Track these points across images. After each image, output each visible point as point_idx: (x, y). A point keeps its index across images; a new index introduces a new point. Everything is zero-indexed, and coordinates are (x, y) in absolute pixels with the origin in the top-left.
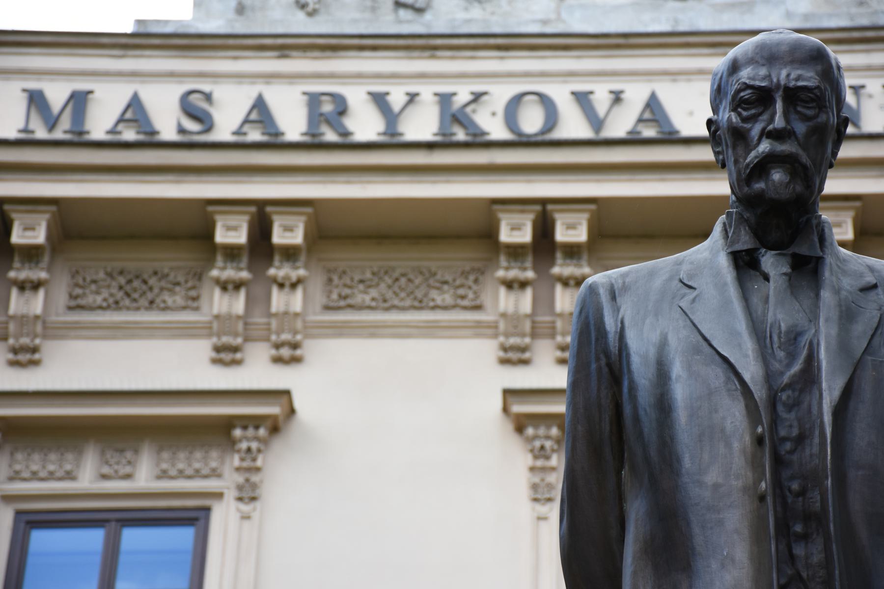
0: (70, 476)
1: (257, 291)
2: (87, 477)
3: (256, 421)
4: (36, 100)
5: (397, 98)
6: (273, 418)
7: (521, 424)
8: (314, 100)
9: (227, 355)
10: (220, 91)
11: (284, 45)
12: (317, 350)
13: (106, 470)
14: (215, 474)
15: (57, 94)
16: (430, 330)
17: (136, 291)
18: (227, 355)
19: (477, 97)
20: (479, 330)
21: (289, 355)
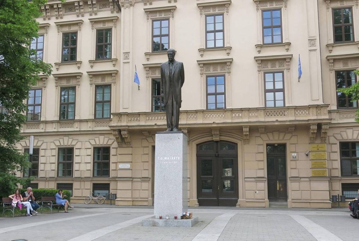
0: (156, 16)
2: (158, 16)
3: (173, 9)
6: (174, 9)
7: (199, 7)
13: (159, 15)
14: (170, 15)
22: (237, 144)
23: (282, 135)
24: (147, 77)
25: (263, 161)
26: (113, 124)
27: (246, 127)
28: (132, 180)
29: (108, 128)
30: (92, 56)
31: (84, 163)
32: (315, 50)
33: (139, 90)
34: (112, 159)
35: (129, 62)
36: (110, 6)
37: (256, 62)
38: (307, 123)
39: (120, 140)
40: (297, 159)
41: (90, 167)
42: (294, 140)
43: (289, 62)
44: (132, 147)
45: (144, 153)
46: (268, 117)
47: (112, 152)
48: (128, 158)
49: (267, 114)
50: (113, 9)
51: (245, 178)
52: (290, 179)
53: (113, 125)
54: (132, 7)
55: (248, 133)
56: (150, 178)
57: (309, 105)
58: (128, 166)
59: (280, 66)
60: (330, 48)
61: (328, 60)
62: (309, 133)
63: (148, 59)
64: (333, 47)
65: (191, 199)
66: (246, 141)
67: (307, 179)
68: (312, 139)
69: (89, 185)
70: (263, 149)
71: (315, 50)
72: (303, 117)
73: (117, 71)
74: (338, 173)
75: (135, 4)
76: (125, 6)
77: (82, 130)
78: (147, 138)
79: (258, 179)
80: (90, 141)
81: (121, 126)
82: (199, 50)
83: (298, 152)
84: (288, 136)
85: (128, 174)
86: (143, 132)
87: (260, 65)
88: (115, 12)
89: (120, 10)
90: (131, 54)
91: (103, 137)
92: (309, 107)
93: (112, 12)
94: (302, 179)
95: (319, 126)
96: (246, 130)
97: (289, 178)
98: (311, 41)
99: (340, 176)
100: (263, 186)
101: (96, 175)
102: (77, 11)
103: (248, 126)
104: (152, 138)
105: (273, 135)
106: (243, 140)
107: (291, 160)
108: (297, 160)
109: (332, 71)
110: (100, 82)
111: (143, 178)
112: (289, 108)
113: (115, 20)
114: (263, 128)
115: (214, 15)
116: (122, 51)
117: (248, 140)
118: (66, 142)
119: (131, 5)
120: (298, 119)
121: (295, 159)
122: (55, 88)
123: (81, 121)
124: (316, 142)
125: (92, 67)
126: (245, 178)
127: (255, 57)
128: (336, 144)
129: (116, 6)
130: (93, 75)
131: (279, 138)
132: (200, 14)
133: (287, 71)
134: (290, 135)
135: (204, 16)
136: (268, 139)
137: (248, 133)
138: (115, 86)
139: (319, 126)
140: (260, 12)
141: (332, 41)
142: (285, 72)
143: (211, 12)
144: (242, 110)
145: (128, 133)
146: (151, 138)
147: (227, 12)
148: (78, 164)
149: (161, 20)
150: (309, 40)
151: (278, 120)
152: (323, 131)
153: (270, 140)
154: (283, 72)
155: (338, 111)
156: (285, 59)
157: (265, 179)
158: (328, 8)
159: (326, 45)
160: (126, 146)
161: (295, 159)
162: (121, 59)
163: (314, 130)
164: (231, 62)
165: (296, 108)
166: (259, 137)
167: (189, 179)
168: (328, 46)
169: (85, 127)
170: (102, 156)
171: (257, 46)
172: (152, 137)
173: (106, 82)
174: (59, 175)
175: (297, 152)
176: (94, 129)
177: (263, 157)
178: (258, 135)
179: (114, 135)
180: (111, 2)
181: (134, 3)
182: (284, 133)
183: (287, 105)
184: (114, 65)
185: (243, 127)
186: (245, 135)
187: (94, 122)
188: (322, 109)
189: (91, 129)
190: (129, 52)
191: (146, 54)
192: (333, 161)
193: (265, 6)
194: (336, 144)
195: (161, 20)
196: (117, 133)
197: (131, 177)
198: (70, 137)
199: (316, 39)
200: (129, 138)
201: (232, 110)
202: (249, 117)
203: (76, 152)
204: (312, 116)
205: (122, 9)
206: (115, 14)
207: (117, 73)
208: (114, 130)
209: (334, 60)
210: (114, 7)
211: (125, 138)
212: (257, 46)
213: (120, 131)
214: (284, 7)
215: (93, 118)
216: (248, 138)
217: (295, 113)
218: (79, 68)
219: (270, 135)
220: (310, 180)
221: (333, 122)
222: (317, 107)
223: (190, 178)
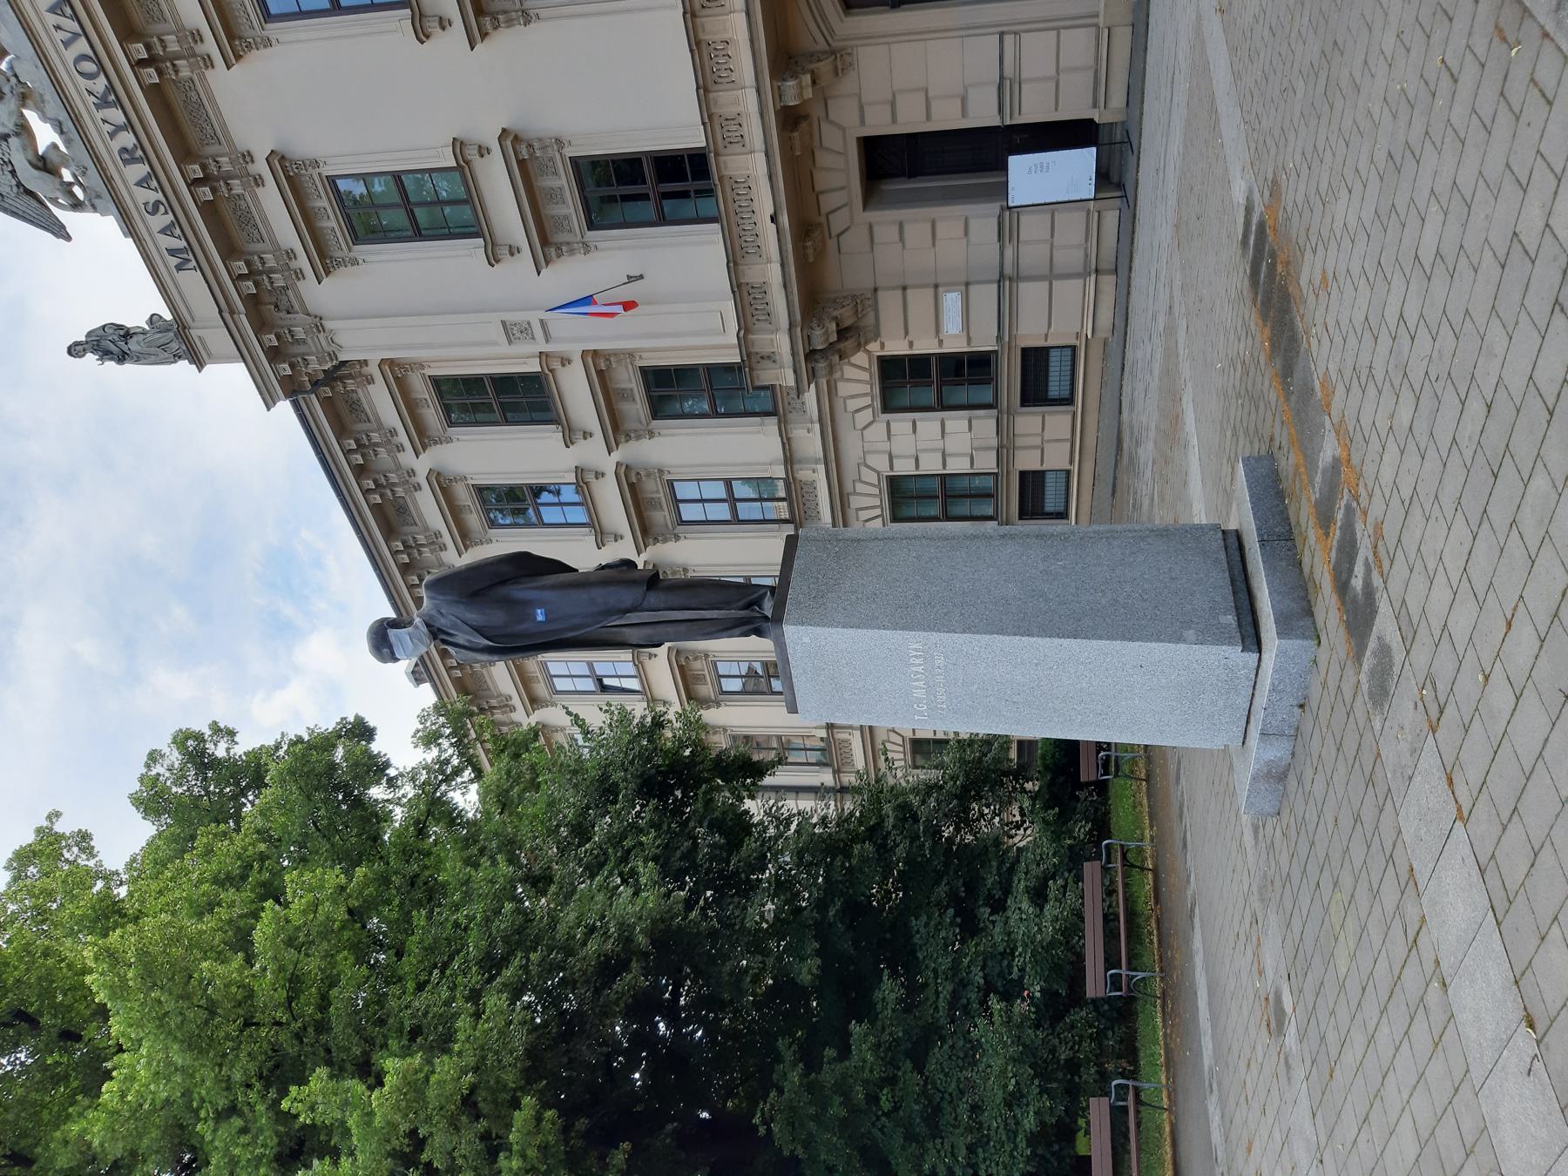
1: (227, 178)
4: (179, 268)
8: (126, 162)
9: (259, 181)
10: (141, 202)
11: (108, 181)
15: (173, 261)
16: (212, 100)
17: (246, 219)
18: (259, 181)
19: (90, 93)
21: (248, 157)
24: (586, 248)
26: (789, 380)
29: (810, 396)
30: (549, 437)
31: (948, 442)
33: (641, 277)
34: (925, 346)
35: (541, 321)
41: (957, 422)
44: (876, 290)
45: (897, 238)
47: (896, 347)
53: (791, 382)
54: (328, 325)
65: (1101, 21)
69: (1029, 422)
75: (311, 309)
76: (329, 349)
77: (821, 455)
80: (860, 425)
81: (794, 354)
85: (985, 297)
86: (811, 259)
90: (510, 317)
91: (840, 385)
101: (986, 394)
102: (400, 491)
110: (639, 405)
113: (397, 373)
116: (504, 348)
118: (869, 502)
119: (320, 328)
122: (682, 542)
123: (789, 460)
125: (587, 435)
130: (616, 429)
132: (269, 50)
135: (273, 29)
138: (644, 355)
148: (948, 460)
160: (872, 315)
167: (1006, 37)
169: (809, 441)
170: (911, 382)
173: (633, 385)
174: (990, 511)
176: (815, 417)
179: (831, 372)
187: (790, 416)
189: (817, 426)
190: (503, 323)
197: (995, 286)
198: (848, 487)
203: (904, 468)
205: (343, 357)
210: (350, 376)
213: (811, 355)
215: (774, 420)
218: (599, 475)
223: (1002, 34)
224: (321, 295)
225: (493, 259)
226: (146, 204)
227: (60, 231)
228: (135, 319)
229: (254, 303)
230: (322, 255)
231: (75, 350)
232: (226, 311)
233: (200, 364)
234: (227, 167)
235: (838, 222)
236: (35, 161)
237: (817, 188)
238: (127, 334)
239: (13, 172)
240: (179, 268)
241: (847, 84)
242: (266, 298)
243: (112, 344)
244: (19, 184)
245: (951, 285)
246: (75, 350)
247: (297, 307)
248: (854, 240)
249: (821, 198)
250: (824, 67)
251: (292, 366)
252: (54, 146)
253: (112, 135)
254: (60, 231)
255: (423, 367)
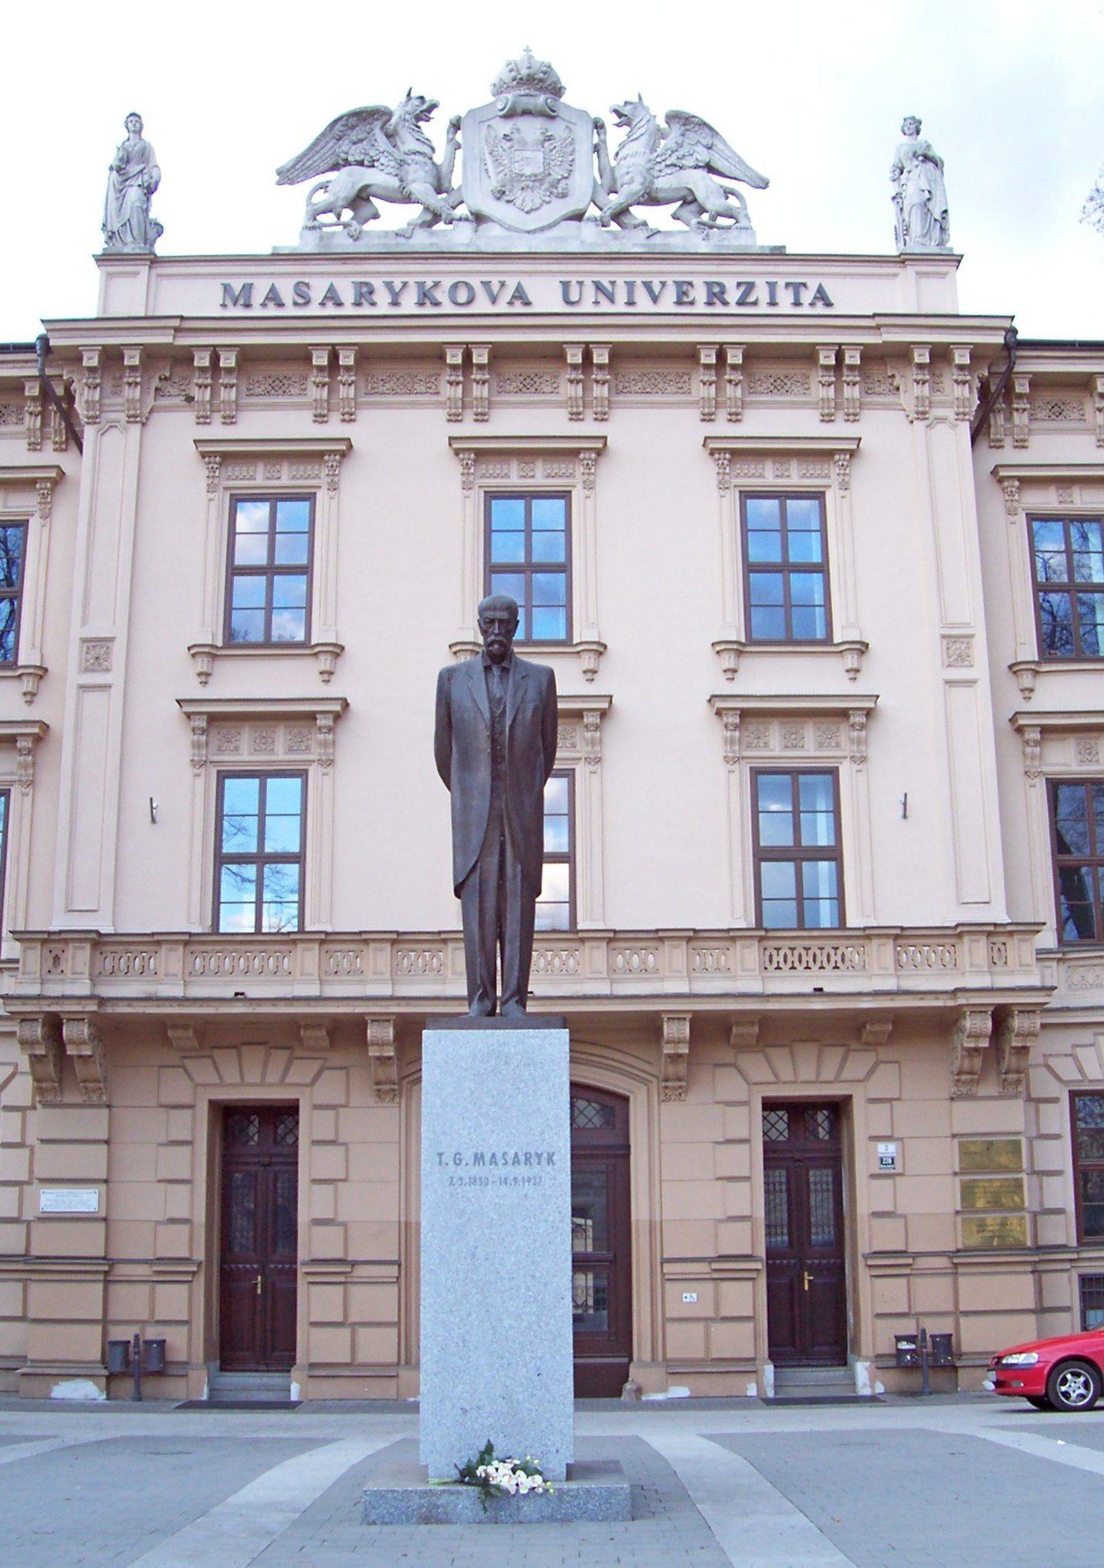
0: (252, 478)
2: (260, 477)
3: (335, 452)
5: (398, 286)
9: (320, 418)
10: (312, 281)
12: (364, 416)
14: (317, 477)
15: (237, 285)
17: (278, 387)
18: (320, 418)
19: (436, 284)
20: (439, 405)
21: (349, 418)
22: (626, 1099)
23: (833, 1056)
25: (748, 1178)
27: (676, 1017)
28: (106, 1273)
32: (970, 683)
36: (27, 416)
37: (715, 718)
38: (951, 1003)
39: (50, 1069)
40: (899, 1170)
42: (884, 1082)
43: (863, 727)
46: (778, 973)
48: (94, 1160)
49: (775, 960)
50: (38, 433)
51: (664, 1261)
52: (870, 1262)
55: (684, 1050)
56: (199, 1264)
57: (957, 925)
58: (88, 1200)
59: (820, 745)
60: (1027, 680)
61: (1020, 730)
62: (954, 1049)
63: (205, 677)
64: (1036, 673)
66: (669, 1084)
67: (943, 1262)
68: (964, 1077)
70: (750, 1124)
71: (970, 683)
72: (930, 979)
73: (45, 727)
74: (1063, 1230)
75: (155, 416)
78: (188, 1063)
79: (723, 1267)
82: (455, 649)
83: (901, 1139)
84: (858, 1064)
85: (89, 1242)
87: (737, 734)
88: (49, 446)
89: (74, 439)
90: (118, 651)
92: (958, 933)
93: (34, 447)
94: (923, 1263)
95: (1001, 1016)
96: (677, 1031)
97: (866, 1257)
98: (955, 645)
99: (1074, 1243)
100: (748, 1298)
103: (690, 1016)
104: (214, 1062)
105: (792, 1054)
106: (655, 1081)
107: (873, 1176)
108: (901, 1175)
109: (1037, 780)
111: (160, 1260)
112: (868, 934)
114: (752, 1023)
115: (529, 496)
116: (77, 632)
117: (679, 1079)
120: (908, 984)
121: (888, 1171)
124: (983, 1090)
126: (664, 1261)
127: (714, 696)
128: (1055, 1100)
129: (55, 420)
131: (818, 1074)
132: (459, 485)
133: (855, 767)
134: (869, 1058)
136: (772, 1078)
137: (684, 1050)
138: (28, 800)
139: (1001, 1016)
140: (732, 499)
141: (1030, 651)
142: (845, 771)
143: (513, 476)
144: (658, 937)
145: (93, 1037)
146: (208, 1061)
147: (589, 486)
149: (274, 499)
150: (943, 637)
151: (821, 990)
152: (1016, 1042)
153: (778, 1082)
154: (833, 772)
155: (1064, 953)
156: (843, 714)
157: (759, 1266)
158: (1011, 512)
159: (1010, 667)
161: (888, 1171)
162: (67, 668)
163: (977, 1036)
164: (603, 714)
165: (901, 936)
166: (733, 1071)
168: (1015, 669)
171: (723, 647)
172: (211, 1057)
175: (898, 1139)
177: (750, 1160)
178: (727, 1055)
180: (34, 399)
181: (150, 412)
182: (841, 1050)
183: (852, 921)
184: (30, 697)
185: (665, 1017)
186: (669, 1056)
188: (1012, 943)
190: (111, 640)
191: (193, 651)
192: (1045, 1179)
193: (753, 476)
194: (1055, 1100)
195: (274, 499)
196: (38, 1031)
199: (972, 636)
200: (97, 1060)
201: (613, 938)
202: (691, 973)
204: (970, 973)
205: (89, 434)
206: (49, 456)
207: (42, 735)
208: (25, 1019)
209: (1045, 730)
210: (44, 424)
211: (81, 1057)
212: (723, 647)
214: (835, 486)
216: (682, 1069)
217: (899, 964)
219: (780, 1057)
220: (956, 1265)
221: (1054, 1002)
222: (992, 932)
224: (177, 433)
225: (196, 651)
226: (307, 285)
227: (288, 175)
228: (159, 209)
229: (182, 358)
230: (227, 458)
231: (135, 124)
232: (182, 324)
233: (102, 259)
234: (343, 392)
235: (203, 1071)
236: (369, 190)
237: (244, 1048)
238: (149, 190)
239: (361, 163)
240: (227, 288)
241: (363, 1095)
242: (180, 371)
243: (134, 168)
244: (347, 163)
245: (108, 1200)
246: (135, 124)
247: (164, 402)
248: (177, 1088)
249: (233, 1052)
250: (393, 1072)
251: (91, 370)
252: (376, 216)
253: (389, 285)
254: (288, 175)
255: (46, 516)
